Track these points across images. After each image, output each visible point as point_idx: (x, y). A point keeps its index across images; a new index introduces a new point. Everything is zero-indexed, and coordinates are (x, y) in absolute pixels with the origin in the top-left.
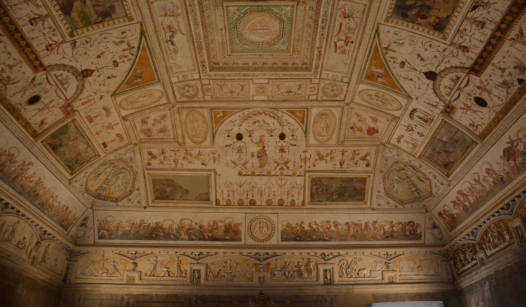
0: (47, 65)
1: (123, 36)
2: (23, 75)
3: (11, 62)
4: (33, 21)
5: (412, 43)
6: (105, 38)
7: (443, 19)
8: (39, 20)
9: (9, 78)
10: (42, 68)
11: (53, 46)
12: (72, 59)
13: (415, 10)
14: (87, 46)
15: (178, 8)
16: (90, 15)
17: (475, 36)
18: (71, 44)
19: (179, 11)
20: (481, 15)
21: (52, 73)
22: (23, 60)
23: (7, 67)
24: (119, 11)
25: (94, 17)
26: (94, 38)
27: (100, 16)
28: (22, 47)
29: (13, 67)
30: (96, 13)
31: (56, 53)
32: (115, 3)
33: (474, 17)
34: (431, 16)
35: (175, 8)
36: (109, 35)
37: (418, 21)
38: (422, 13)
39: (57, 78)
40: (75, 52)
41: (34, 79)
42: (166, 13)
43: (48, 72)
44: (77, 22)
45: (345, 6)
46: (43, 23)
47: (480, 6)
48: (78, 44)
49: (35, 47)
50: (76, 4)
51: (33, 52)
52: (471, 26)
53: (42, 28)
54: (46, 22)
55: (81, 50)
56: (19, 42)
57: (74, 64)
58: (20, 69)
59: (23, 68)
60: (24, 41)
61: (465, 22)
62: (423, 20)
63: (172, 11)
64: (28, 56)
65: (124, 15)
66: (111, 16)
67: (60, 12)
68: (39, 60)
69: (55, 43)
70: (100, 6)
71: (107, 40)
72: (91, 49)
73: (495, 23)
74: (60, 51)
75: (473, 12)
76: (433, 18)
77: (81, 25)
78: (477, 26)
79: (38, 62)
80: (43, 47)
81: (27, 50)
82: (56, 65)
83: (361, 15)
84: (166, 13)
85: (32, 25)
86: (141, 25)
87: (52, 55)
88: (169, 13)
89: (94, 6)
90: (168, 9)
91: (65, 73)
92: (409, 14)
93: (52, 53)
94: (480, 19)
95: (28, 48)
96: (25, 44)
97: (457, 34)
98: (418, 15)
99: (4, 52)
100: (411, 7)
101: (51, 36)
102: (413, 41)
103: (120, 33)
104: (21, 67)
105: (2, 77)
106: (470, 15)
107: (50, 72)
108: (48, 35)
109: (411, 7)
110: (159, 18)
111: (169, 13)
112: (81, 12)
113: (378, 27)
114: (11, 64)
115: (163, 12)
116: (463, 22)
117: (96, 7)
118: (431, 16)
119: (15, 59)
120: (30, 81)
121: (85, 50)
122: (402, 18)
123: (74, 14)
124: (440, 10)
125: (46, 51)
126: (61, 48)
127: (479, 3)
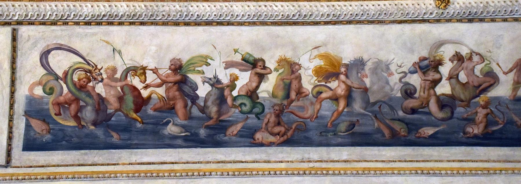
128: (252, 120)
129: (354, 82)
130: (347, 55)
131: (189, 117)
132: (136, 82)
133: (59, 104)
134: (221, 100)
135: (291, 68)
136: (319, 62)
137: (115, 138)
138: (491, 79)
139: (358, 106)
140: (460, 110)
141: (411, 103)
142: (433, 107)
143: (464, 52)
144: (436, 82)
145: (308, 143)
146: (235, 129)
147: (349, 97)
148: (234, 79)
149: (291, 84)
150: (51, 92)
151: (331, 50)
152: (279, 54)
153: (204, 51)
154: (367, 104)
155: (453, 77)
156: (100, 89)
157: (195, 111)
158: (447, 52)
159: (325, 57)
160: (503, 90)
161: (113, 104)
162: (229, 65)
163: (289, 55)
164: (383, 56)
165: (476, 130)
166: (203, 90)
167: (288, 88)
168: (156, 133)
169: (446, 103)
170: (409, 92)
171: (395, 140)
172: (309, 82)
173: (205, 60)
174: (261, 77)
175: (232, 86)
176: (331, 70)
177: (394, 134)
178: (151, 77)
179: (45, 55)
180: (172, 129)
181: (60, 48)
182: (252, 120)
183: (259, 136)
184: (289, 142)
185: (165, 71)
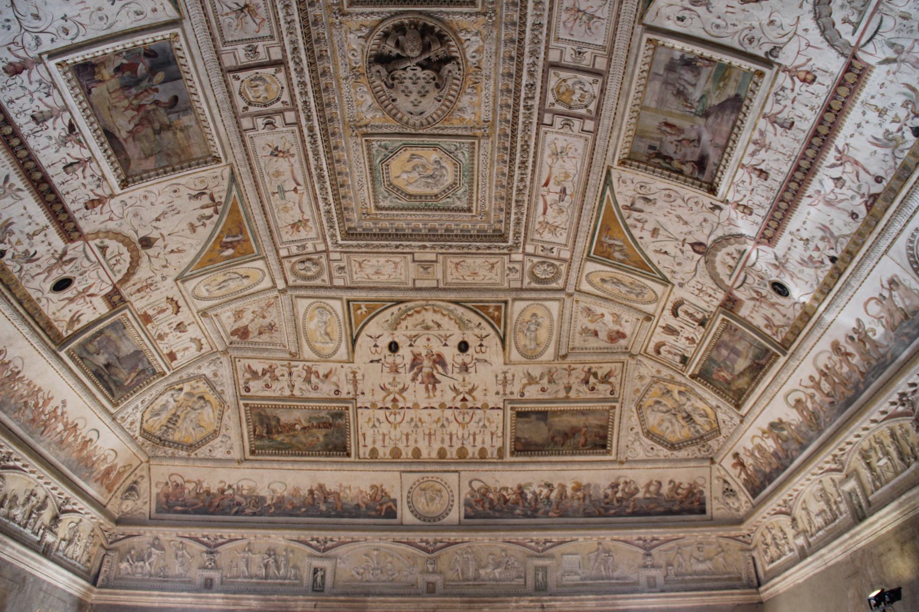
0: (843, 60)
1: (686, 14)
2: (887, 83)
3: (872, 116)
4: (788, 125)
5: (100, 14)
6: (718, 26)
7: (93, 84)
8: (778, 121)
9: (905, 105)
10: (855, 62)
11: (802, 75)
12: (800, 32)
13: (144, 72)
14: (757, 33)
15: (564, 23)
16: (709, 77)
17: (26, 100)
18: (776, 57)
19: (564, 16)
20: (55, 129)
21: (853, 41)
22: (859, 102)
23: (885, 117)
24: (663, 58)
25: (706, 72)
26: (736, 38)
27: (697, 68)
28: (836, 116)
29: (880, 107)
30: (699, 74)
31: (811, 63)
32: (661, 72)
33: (59, 120)
34: (112, 77)
35: (569, 25)
36: (708, 28)
37: (124, 58)
38: (128, 73)
39: (859, 23)
40: (785, 39)
41: (887, 61)
42: (589, 20)
43: (858, 47)
44: (736, 81)
45: (256, 28)
46: (779, 113)
47: (68, 136)
48: (767, 48)
49: (823, 98)
50: (716, 102)
51: (834, 95)
52: (48, 106)
53: (786, 110)
54: (774, 112)
55: (772, 34)
56: (832, 123)
57: (808, 21)
58: (879, 96)
59: (873, 93)
60: (826, 118)
61: (60, 103)
62: (117, 64)
63: (578, 21)
64: (846, 98)
65: (659, 50)
66: (682, 57)
67: (744, 109)
68: (843, 78)
69: (795, 78)
70: (685, 81)
71: (719, 21)
72: (755, 24)
73: (29, 135)
74: (801, 60)
75: (67, 123)
76: (107, 77)
77: (734, 75)
78: (41, 112)
79: (847, 76)
80: (814, 87)
81: (836, 105)
82: (832, 46)
83: (221, 22)
84: (589, 20)
85: (793, 123)
86: (642, 17)
87: (820, 64)
88: (584, 18)
89: (694, 85)
90: (583, 26)
91: (837, 16)
92: (147, 61)
93: (814, 68)
94: (49, 123)
95: (833, 106)
96: (828, 114)
97: (50, 80)
98: (133, 67)
99: (861, 134)
100: (152, 71)
101: (788, 92)
102: (101, 19)
103: (687, 22)
104: (873, 97)
105: (908, 115)
106: (67, 116)
107: (853, 44)
108: (791, 96)
109: (152, 71)
110: (606, 16)
111: (584, 18)
112: (718, 88)
113: (178, 10)
114: (877, 114)
115: (595, 24)
116: (64, 100)
117: (693, 82)
118: (112, 77)
119: (864, 113)
120: (894, 66)
121: (767, 29)
122: (152, 48)
123: (731, 92)
124: (110, 93)
125: (819, 79)
126: (796, 64)
127: (73, 137)
128: (548, 508)
129: (586, 492)
130: (584, 482)
131: (524, 506)
132: (504, 493)
133: (476, 501)
134: (536, 500)
135: (563, 487)
136: (574, 485)
137: (497, 514)
138: (637, 490)
139: (587, 501)
140: (624, 503)
141: (607, 500)
142: (615, 502)
143: (628, 480)
144: (616, 492)
145: (568, 516)
146: (541, 511)
147: (584, 498)
148: (541, 491)
149: (562, 495)
150: (473, 496)
151: (579, 480)
152: (558, 482)
153: (530, 481)
154: (591, 501)
155: (623, 490)
156: (491, 496)
157: (526, 504)
158: (622, 480)
159: (576, 483)
160: (640, 495)
161: (496, 502)
162: (540, 486)
163: (562, 482)
164: (598, 482)
165: (629, 510)
166: (529, 496)
167: (561, 495)
168: (512, 513)
169: (619, 500)
170: (606, 496)
171: (600, 515)
172: (569, 492)
173: (530, 484)
174: (551, 491)
175: (540, 494)
176: (578, 488)
177: (600, 512)
178: (510, 491)
179: (470, 482)
180: (518, 512)
181: (476, 480)
182: (548, 508)
183: (550, 514)
184: (561, 516)
185: (515, 488)
